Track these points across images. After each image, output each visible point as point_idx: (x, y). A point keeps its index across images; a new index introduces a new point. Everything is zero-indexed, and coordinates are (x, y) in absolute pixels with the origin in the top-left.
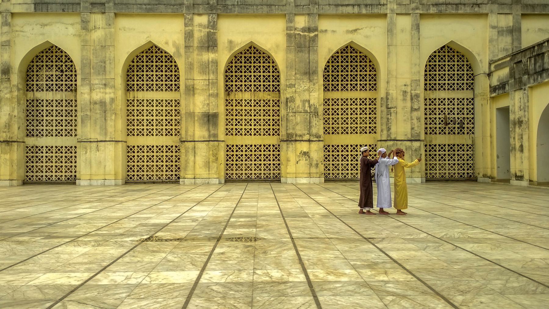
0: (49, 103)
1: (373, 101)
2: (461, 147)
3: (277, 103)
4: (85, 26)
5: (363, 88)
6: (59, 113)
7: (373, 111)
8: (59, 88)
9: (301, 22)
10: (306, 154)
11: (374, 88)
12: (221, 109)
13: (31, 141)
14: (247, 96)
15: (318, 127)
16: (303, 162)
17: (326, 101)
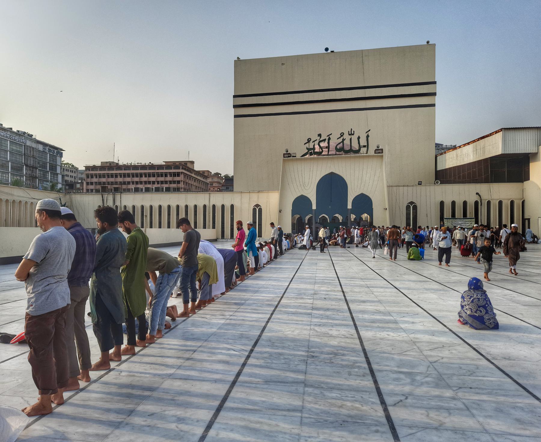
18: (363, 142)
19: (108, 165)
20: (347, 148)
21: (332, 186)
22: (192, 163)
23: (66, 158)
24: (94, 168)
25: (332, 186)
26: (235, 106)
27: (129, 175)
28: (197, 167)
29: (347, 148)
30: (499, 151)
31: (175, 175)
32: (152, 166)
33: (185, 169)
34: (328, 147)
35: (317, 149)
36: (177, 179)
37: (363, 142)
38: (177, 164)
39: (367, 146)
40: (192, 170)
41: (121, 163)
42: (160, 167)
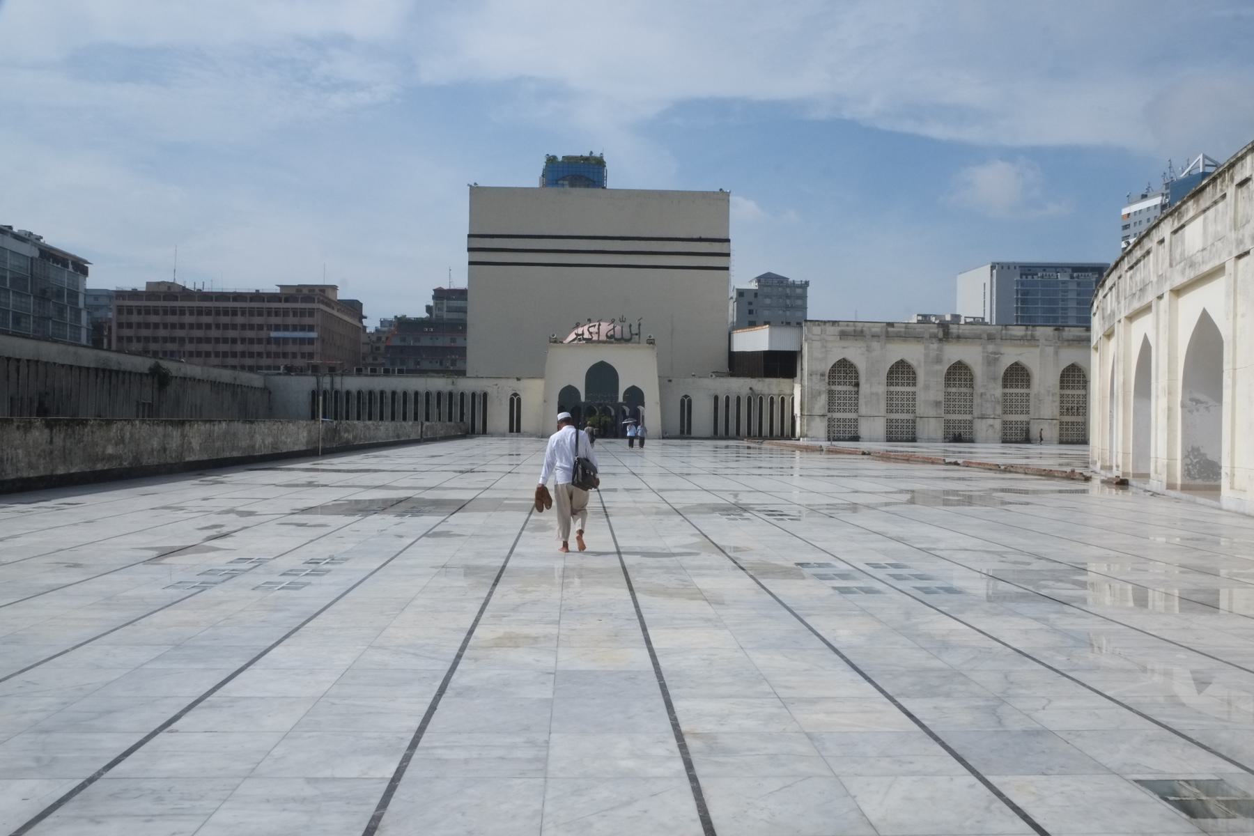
0: (839, 392)
1: (1028, 395)
2: (1078, 423)
3: (972, 395)
4: (869, 349)
5: (1022, 387)
6: (845, 399)
7: (1028, 401)
8: (845, 383)
9: (991, 348)
10: (991, 426)
11: (1028, 387)
12: (941, 397)
13: (829, 415)
14: (953, 390)
15: (999, 410)
16: (990, 431)
17: (1005, 395)
18: (635, 330)
19: (164, 289)
20: (618, 335)
21: (602, 375)
22: (334, 288)
23: (96, 281)
24: (134, 294)
25: (602, 375)
26: (470, 250)
27: (208, 312)
28: (341, 295)
29: (618, 335)
30: (766, 349)
31: (302, 313)
32: (257, 296)
33: (323, 302)
34: (598, 333)
35: (587, 335)
36: (307, 321)
37: (635, 330)
38: (305, 291)
39: (638, 334)
40: (330, 303)
41: (190, 286)
42: (272, 297)
